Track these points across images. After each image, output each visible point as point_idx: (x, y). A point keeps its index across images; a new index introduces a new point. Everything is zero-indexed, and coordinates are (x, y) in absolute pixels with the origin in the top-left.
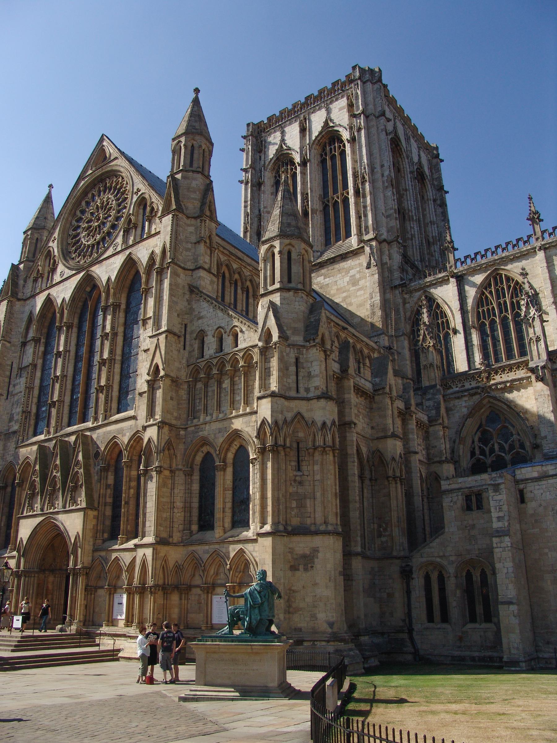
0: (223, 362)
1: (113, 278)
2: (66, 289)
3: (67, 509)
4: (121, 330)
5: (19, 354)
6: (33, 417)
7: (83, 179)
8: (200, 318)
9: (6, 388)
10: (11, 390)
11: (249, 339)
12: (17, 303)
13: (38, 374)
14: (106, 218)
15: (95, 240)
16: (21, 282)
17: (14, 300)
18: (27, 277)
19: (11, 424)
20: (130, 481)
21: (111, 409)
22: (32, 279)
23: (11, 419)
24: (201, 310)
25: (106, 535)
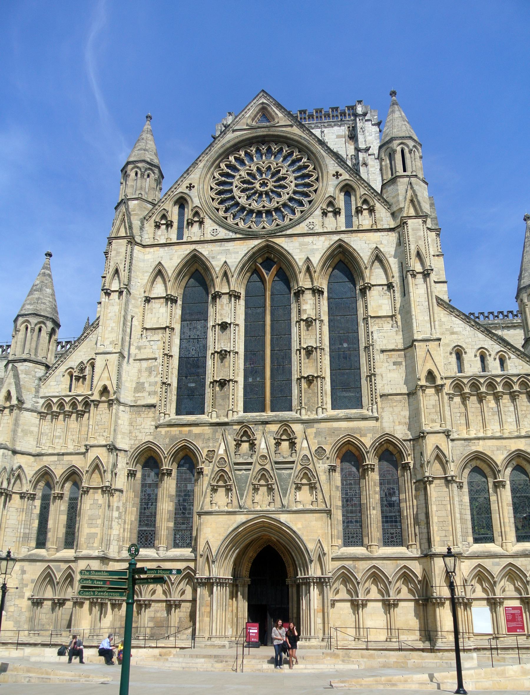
0: (490, 382)
1: (316, 260)
2: (227, 252)
3: (295, 509)
4: (325, 318)
5: (141, 310)
6: (174, 392)
7: (234, 131)
8: (453, 333)
9: (126, 349)
10: (133, 351)
11: (521, 367)
12: (136, 247)
13: (177, 341)
14: (275, 187)
15: (264, 207)
16: (136, 223)
17: (134, 242)
18: (145, 218)
19: (139, 395)
20: (375, 485)
21: (326, 404)
22: (152, 222)
23: (139, 387)
24: (453, 326)
25: (340, 542)
